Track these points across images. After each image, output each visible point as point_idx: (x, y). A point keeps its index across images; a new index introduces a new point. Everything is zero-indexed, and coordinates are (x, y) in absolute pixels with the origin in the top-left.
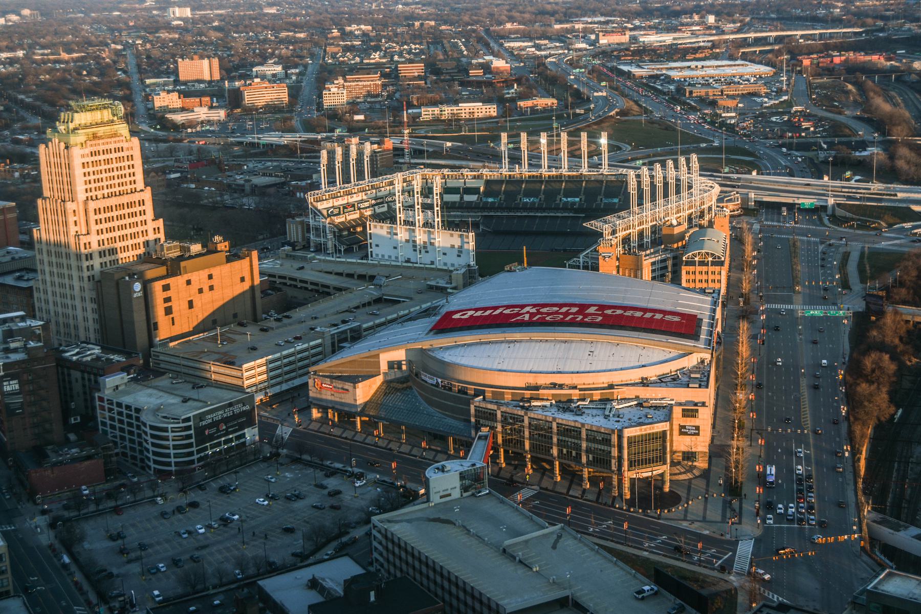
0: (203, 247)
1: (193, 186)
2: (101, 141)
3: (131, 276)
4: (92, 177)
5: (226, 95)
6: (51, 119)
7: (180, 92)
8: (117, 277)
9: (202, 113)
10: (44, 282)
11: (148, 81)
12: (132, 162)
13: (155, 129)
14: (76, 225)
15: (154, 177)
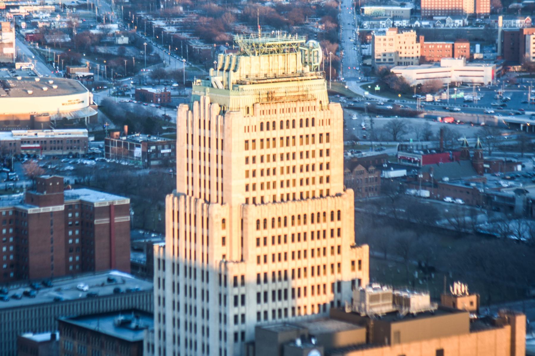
0: (433, 300)
1: (426, 193)
2: (279, 107)
3: (306, 339)
4: (258, 166)
5: (499, 40)
6: (203, 63)
7: (419, 31)
8: (282, 338)
9: (453, 68)
10: (163, 335)
11: (368, 10)
12: (327, 146)
13: (372, 91)
14: (224, 243)
15: (361, 173)
